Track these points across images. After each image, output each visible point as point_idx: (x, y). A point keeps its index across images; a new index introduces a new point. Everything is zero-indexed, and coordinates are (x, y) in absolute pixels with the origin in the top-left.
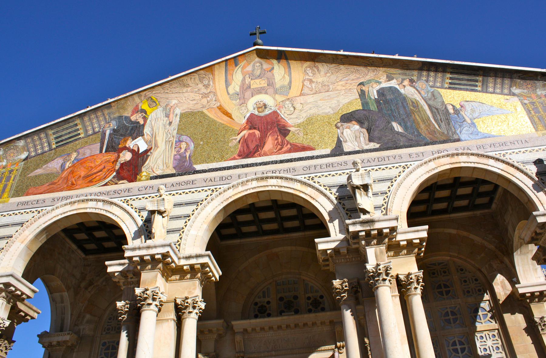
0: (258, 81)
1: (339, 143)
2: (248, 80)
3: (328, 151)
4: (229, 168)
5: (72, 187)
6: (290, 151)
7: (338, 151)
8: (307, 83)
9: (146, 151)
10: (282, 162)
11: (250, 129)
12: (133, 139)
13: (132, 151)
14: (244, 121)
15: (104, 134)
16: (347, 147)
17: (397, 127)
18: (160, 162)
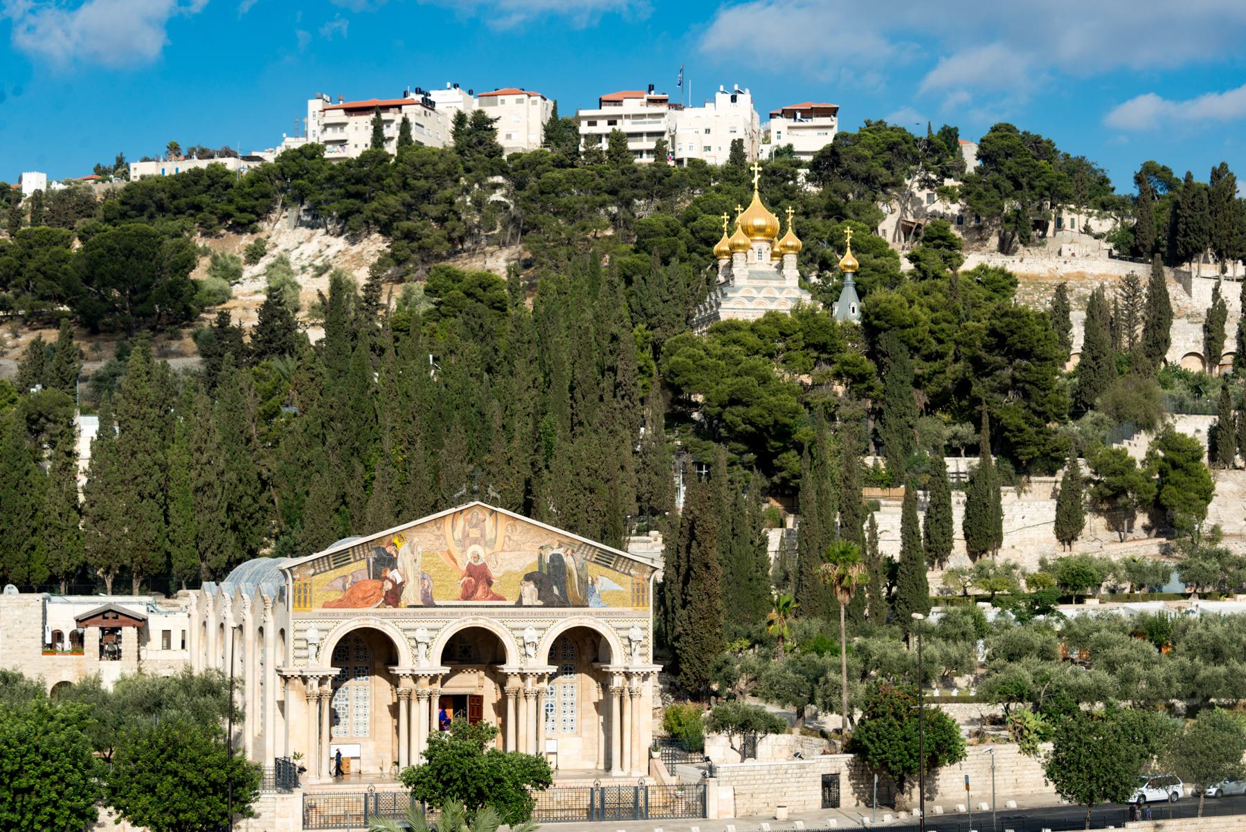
0: (474, 530)
1: (521, 596)
2: (467, 528)
3: (513, 603)
4: (456, 606)
5: (355, 605)
6: (492, 599)
7: (519, 604)
8: (507, 539)
9: (402, 583)
10: (487, 606)
11: (470, 575)
12: (392, 570)
13: (391, 581)
14: (464, 568)
15: (368, 561)
16: (524, 603)
17: (556, 591)
18: (412, 594)
